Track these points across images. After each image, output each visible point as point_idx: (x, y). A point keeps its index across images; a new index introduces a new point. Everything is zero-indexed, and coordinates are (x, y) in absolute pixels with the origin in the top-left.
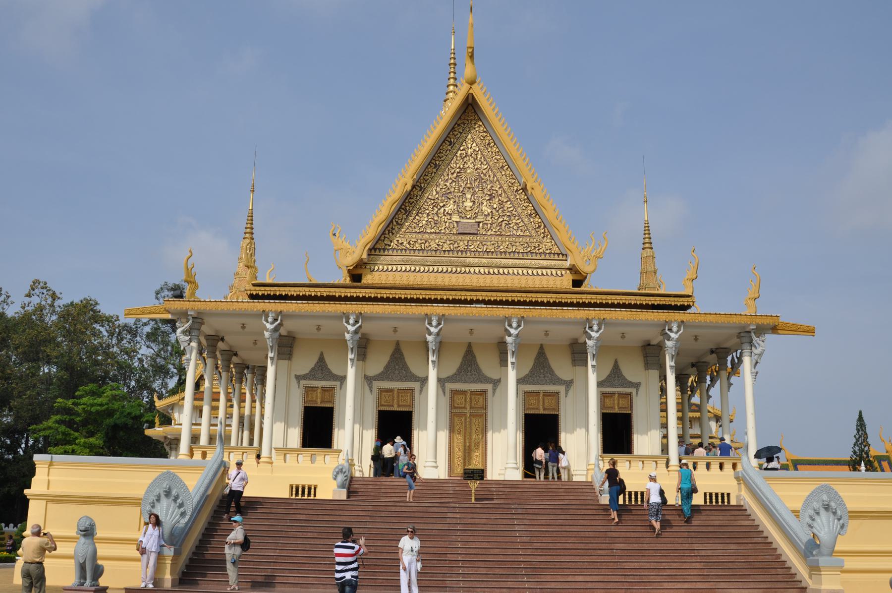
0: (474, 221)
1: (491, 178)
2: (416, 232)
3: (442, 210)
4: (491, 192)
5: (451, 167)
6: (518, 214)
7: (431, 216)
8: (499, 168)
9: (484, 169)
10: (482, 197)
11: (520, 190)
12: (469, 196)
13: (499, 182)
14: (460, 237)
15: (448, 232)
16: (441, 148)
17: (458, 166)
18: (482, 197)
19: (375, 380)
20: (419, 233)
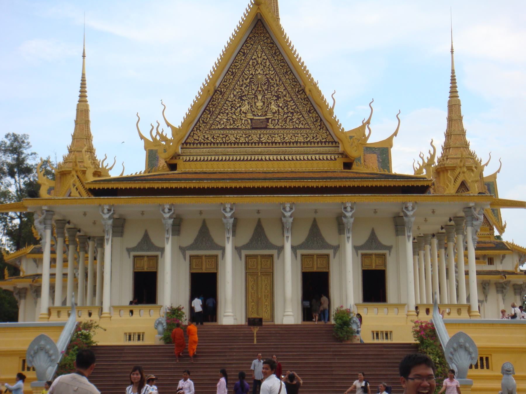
0: (264, 118)
1: (278, 82)
2: (218, 129)
3: (239, 109)
4: (277, 93)
5: (245, 74)
6: (300, 111)
7: (230, 115)
8: (283, 73)
9: (272, 75)
10: (270, 98)
11: (301, 90)
12: (260, 97)
13: (284, 85)
14: (253, 131)
15: (244, 127)
16: (237, 58)
17: (251, 72)
18: (270, 98)
19: (188, 250)
20: (221, 129)
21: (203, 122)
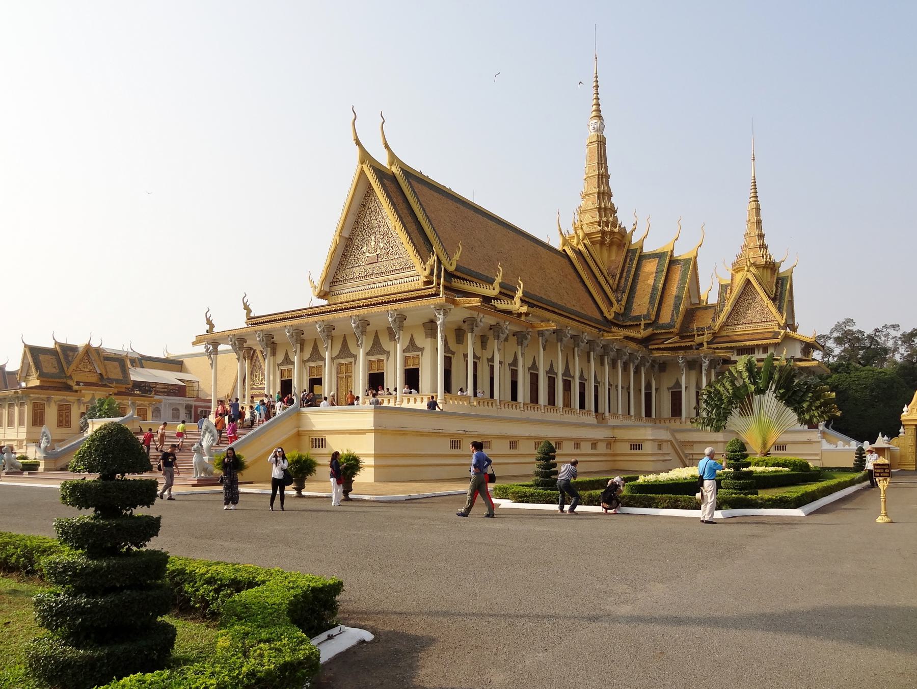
0: (375, 254)
3: (361, 251)
12: (373, 238)
21: (342, 265)
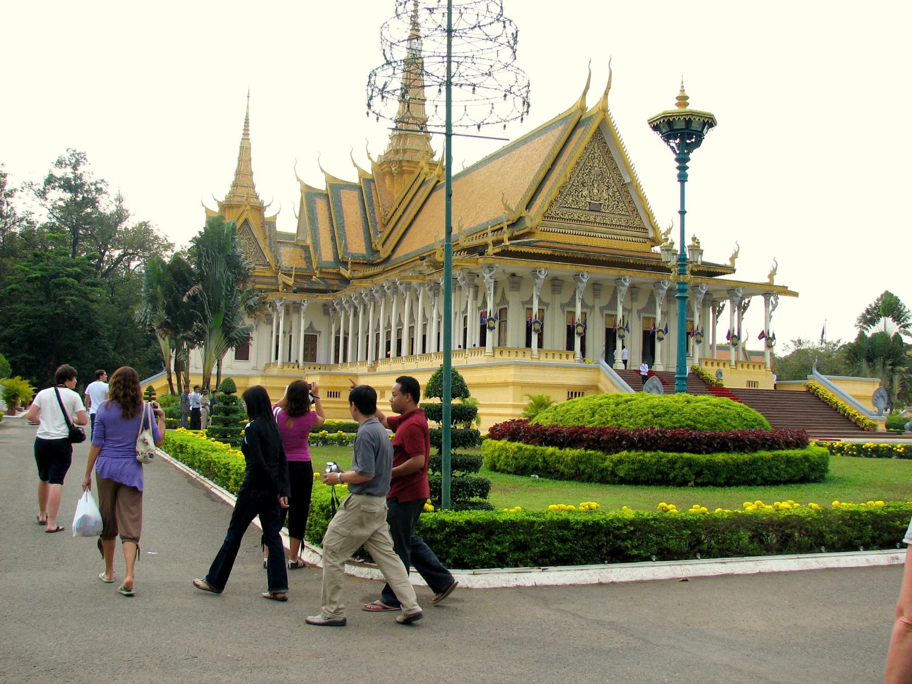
2: (566, 207)
12: (596, 186)
14: (591, 212)
